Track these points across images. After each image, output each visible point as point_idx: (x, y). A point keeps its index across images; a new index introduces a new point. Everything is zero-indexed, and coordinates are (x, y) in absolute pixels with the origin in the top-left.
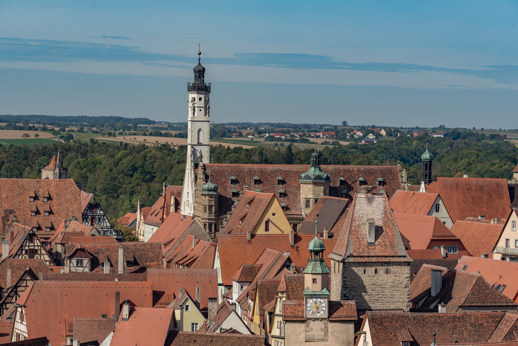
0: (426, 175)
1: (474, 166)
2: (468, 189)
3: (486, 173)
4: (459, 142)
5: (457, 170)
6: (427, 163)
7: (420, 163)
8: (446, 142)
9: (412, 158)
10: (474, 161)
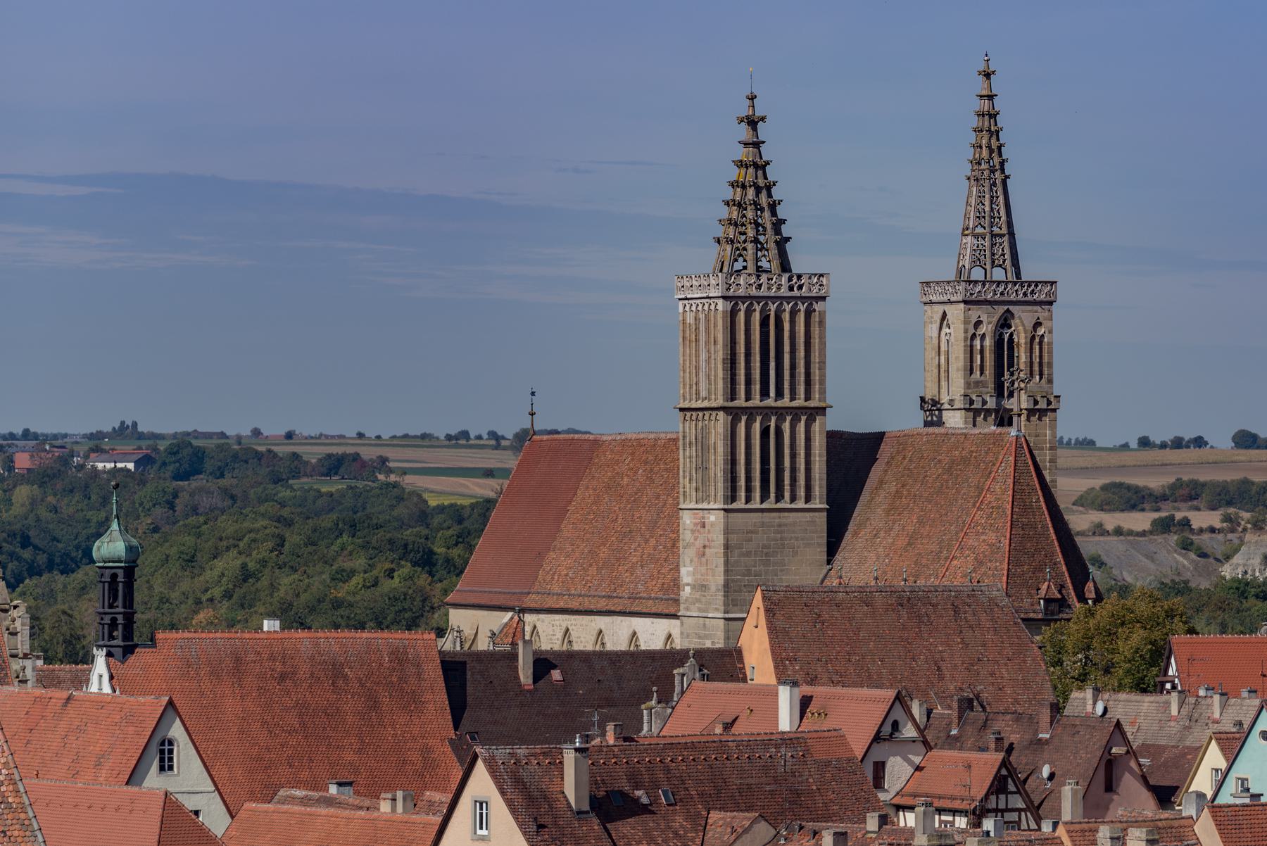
0: (113, 625)
1: (264, 582)
2: (283, 677)
3: (312, 610)
4: (201, 490)
5: (198, 602)
6: (114, 576)
7: (45, 577)
8: (149, 488)
9: (12, 555)
10: (263, 563)
